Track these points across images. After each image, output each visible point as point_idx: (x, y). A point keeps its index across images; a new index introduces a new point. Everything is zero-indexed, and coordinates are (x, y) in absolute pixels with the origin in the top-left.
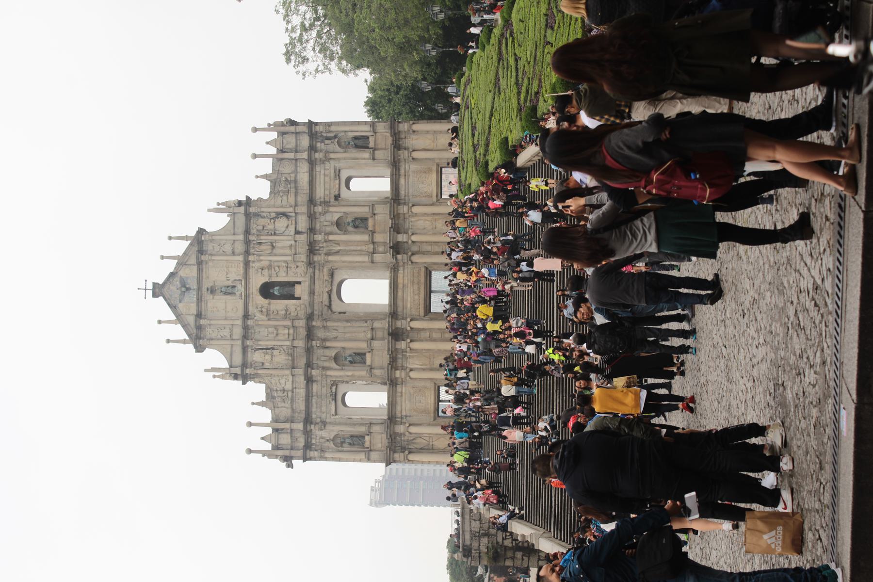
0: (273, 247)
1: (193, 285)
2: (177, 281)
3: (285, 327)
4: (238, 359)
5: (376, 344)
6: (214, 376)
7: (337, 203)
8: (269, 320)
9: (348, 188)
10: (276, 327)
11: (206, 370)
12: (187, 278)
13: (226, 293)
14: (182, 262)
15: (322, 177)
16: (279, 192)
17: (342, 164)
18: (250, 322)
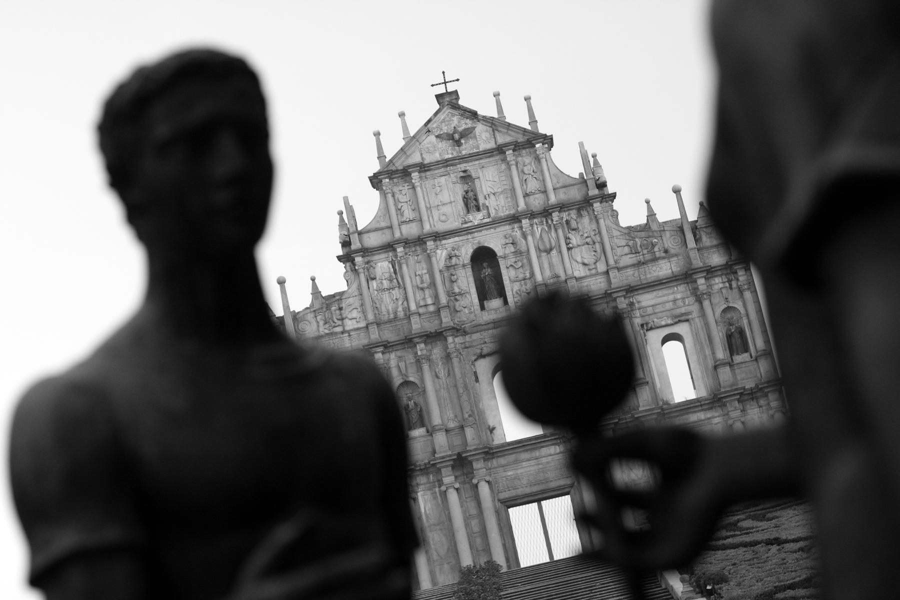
0: (549, 251)
1: (467, 148)
2: (467, 123)
3: (436, 297)
4: (373, 240)
5: (440, 439)
6: (340, 213)
8: (440, 271)
9: (665, 340)
10: (433, 284)
11: (346, 200)
12: (475, 137)
13: (466, 200)
14: (496, 124)
15: (671, 297)
16: (633, 239)
17: (698, 322)
18: (430, 244)
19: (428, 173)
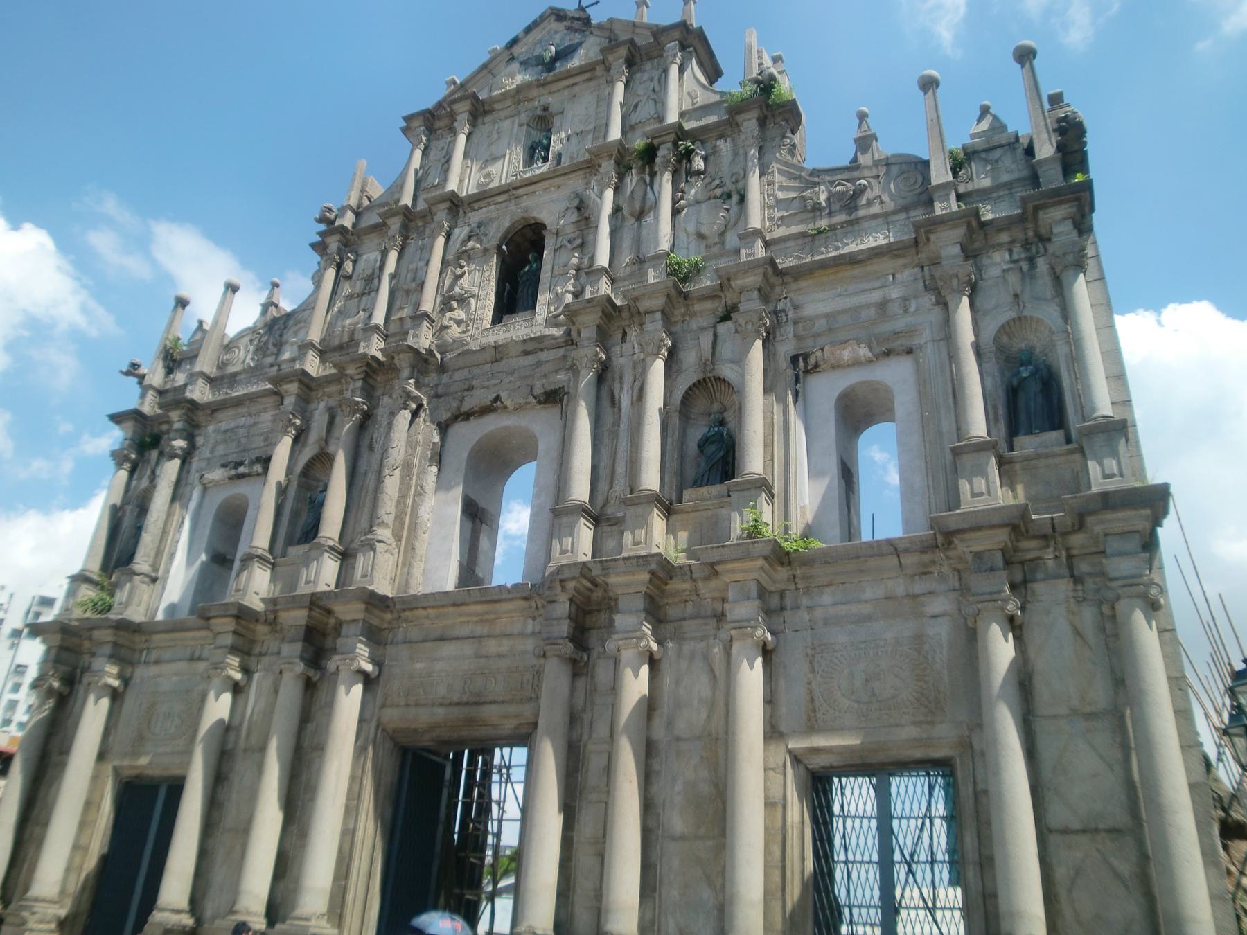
7: (783, 363)
15: (876, 296)
19: (488, 118)
